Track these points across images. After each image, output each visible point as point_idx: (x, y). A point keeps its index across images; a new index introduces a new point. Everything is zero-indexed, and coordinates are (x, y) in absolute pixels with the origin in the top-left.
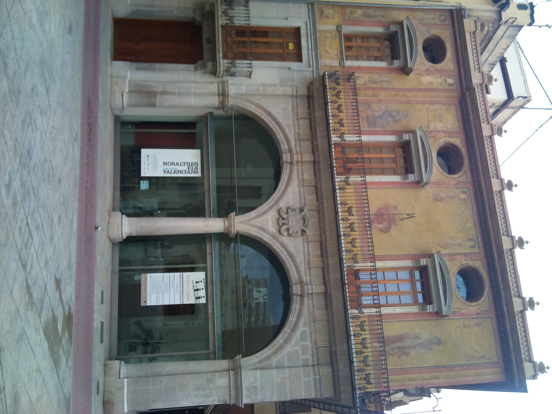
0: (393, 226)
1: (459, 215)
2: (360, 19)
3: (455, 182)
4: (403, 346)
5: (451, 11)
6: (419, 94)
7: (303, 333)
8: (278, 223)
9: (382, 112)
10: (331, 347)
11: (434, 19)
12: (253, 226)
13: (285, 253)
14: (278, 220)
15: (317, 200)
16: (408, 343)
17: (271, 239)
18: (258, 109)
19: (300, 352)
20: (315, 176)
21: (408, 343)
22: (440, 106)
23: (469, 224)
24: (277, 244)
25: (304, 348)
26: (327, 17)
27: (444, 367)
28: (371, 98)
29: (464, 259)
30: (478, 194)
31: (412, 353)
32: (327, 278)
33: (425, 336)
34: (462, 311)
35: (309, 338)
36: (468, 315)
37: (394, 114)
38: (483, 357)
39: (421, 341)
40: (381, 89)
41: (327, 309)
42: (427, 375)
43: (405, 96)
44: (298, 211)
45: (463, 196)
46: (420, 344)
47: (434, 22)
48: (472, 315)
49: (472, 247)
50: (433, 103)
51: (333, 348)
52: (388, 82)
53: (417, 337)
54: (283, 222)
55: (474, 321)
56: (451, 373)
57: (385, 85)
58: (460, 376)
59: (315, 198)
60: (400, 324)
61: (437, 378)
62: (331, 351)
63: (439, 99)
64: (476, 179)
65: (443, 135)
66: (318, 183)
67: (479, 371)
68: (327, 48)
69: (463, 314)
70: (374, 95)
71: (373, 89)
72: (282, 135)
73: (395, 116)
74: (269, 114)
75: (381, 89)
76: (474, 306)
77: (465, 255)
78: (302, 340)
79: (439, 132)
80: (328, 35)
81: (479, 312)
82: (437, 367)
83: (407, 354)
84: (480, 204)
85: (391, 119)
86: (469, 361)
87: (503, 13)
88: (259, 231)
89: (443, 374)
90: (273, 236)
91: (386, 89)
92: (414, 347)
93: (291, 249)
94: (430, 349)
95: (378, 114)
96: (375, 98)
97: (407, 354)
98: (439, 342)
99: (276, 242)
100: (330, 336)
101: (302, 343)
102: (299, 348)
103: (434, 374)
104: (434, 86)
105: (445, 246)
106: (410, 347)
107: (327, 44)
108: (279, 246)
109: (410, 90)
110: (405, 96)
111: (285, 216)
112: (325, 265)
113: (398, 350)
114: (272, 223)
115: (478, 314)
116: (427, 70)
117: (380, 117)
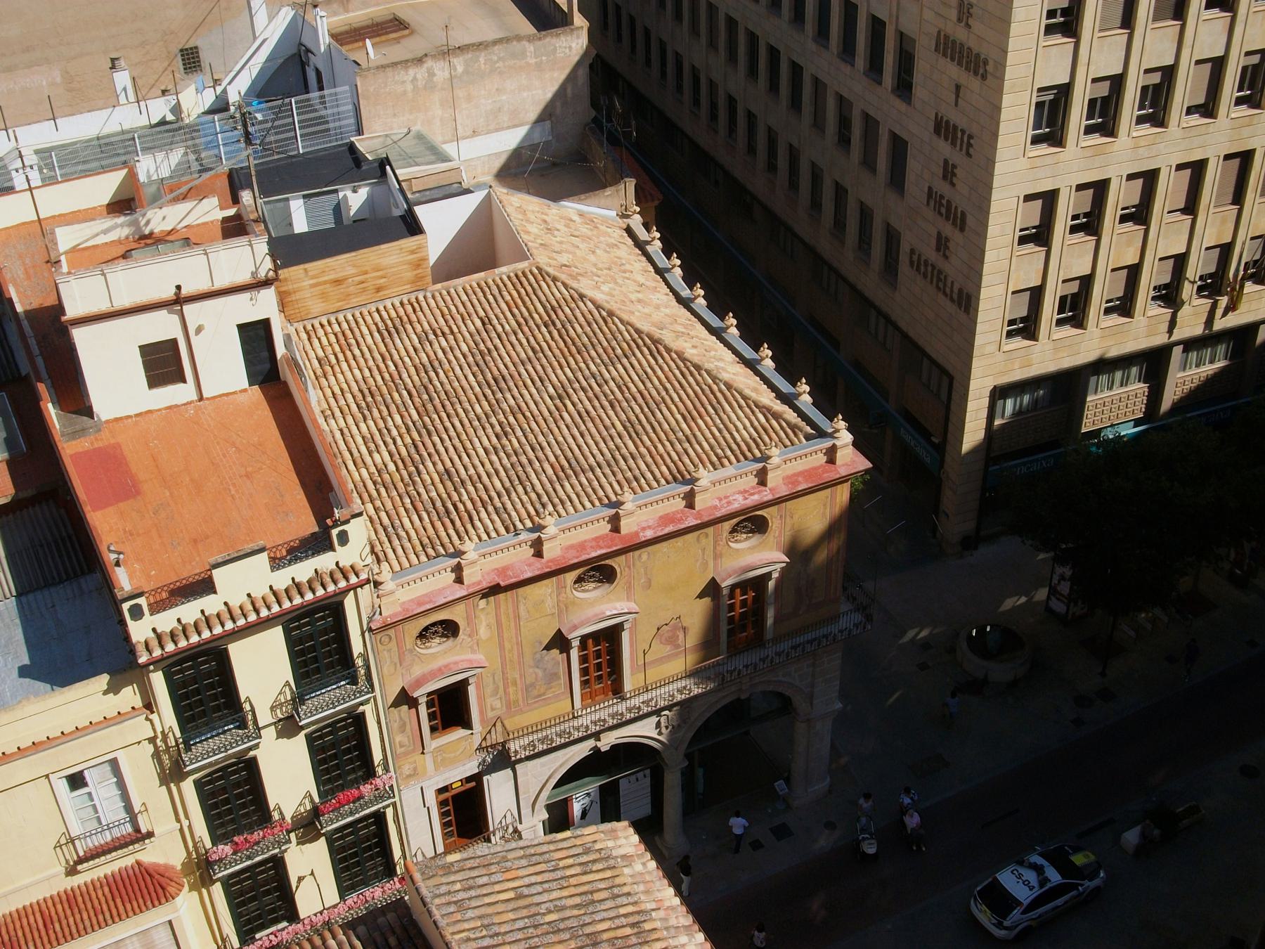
6: (505, 635)
11: (389, 651)
22: (522, 608)
26: (415, 769)
40: (505, 679)
43: (510, 651)
45: (645, 557)
49: (707, 535)
50: (517, 617)
63: (511, 611)
70: (515, 684)
77: (715, 542)
80: (439, 758)
95: (540, 673)
104: (493, 621)
105: (706, 564)
109: (502, 647)
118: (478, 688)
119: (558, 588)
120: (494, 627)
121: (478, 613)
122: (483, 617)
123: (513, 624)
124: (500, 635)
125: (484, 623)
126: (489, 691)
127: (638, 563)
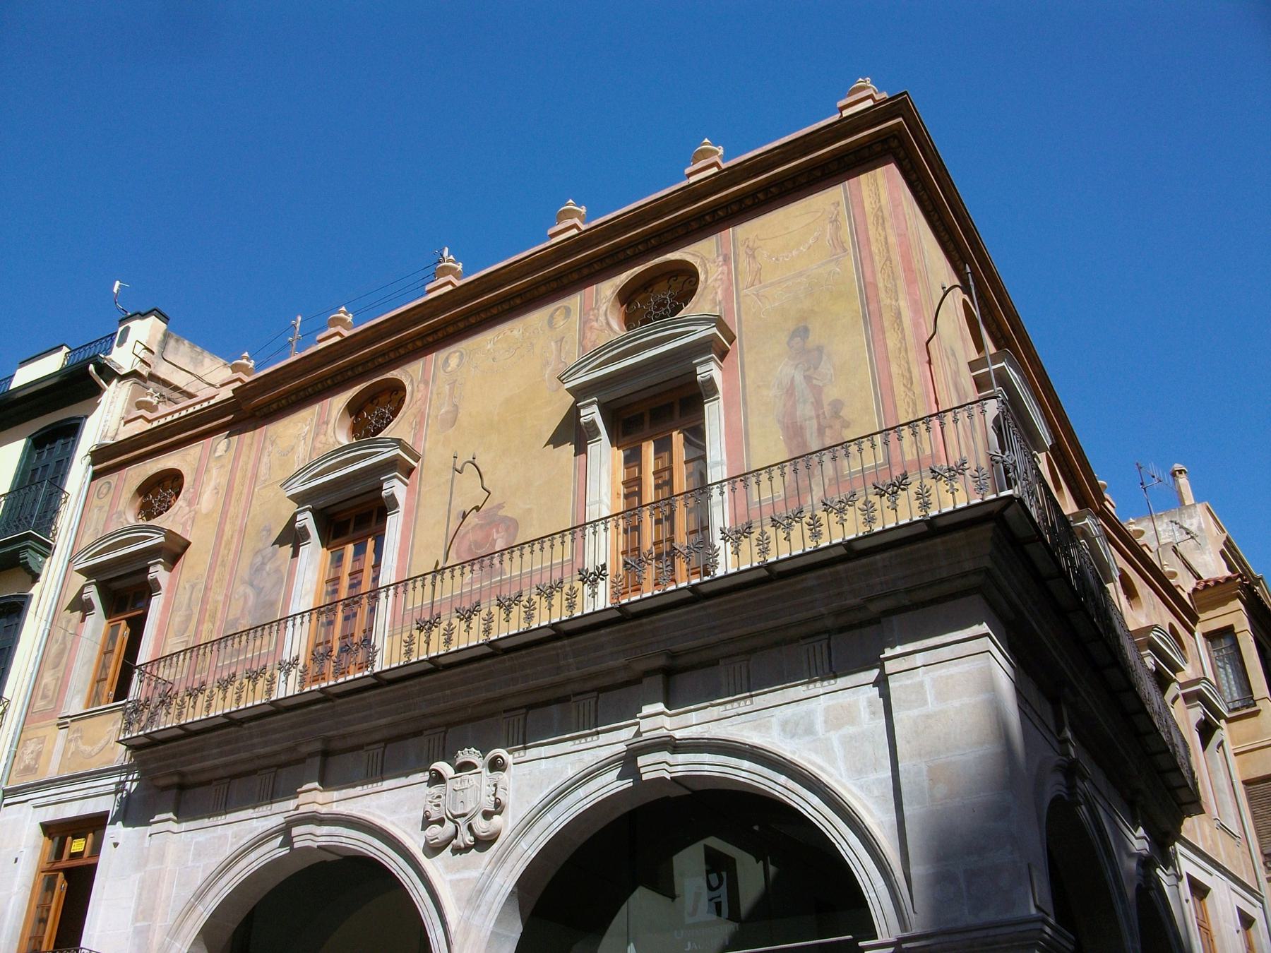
0: (502, 513)
1: (494, 359)
2: (61, 675)
3: (422, 386)
4: (815, 422)
5: (96, 475)
6: (232, 510)
7: (789, 729)
8: (467, 849)
9: (249, 591)
10: (828, 631)
11: (101, 508)
12: (466, 932)
13: (549, 817)
14: (457, 851)
15: (417, 733)
16: (805, 411)
17: (508, 866)
18: (185, 931)
19: (850, 730)
20: (359, 747)
21: (805, 411)
22: (265, 459)
23: (515, 332)
24: (523, 845)
25: (836, 720)
27: (866, 302)
28: (218, 623)
29: (595, 324)
30: (451, 330)
31: (832, 393)
32: (622, 676)
33: (786, 370)
34: (720, 297)
35: (803, 706)
36: (730, 280)
37: (259, 560)
38: (834, 221)
39: (799, 378)
40: (204, 601)
41: (714, 663)
42: (892, 341)
44: (435, 790)
45: (454, 362)
46: (808, 379)
47: (107, 508)
48: (729, 273)
49: (568, 311)
50: (255, 476)
51: (829, 622)
52: (193, 587)
53: (790, 391)
54: (463, 829)
55: (744, 263)
56: (881, 285)
57: (198, 594)
58: (889, 259)
59: (416, 740)
60: (754, 441)
61: (899, 315)
62: (841, 630)
63: (250, 466)
64: (419, 343)
65: (322, 438)
66: (377, 736)
67: (870, 219)
68: (96, 749)
69: (728, 292)
70: (213, 617)
71: (200, 622)
72: (253, 856)
73: (263, 558)
74: (200, 895)
75: (204, 601)
76: (706, 273)
78: (810, 730)
79: (313, 448)
80: (72, 747)
81: (721, 258)
82: (867, 318)
83: (837, 406)
84: (472, 320)
85: (267, 568)
86: (845, 250)
87: (122, 372)
88: (483, 909)
89: (885, 300)
90: (501, 860)
91: (207, 589)
92: (818, 392)
93: (537, 798)
94: (820, 349)
96: (219, 615)
97: (837, 406)
98: (802, 332)
99: (519, 850)
100: (792, 641)
101: (819, 726)
102: (834, 737)
103: (886, 324)
104: (224, 481)
106: (818, 404)
107: (88, 748)
108: (530, 838)
109: (220, 536)
110: (229, 543)
111: (449, 827)
112: (589, 686)
113: (828, 432)
114: (466, 867)
115: (726, 260)
116: (190, 504)
117: (259, 591)
118: (166, 607)
119: (318, 425)
120: (222, 493)
121: (212, 464)
122: (214, 472)
123: (245, 491)
124: (224, 512)
125: (212, 484)
126: (178, 619)
127: (441, 374)
